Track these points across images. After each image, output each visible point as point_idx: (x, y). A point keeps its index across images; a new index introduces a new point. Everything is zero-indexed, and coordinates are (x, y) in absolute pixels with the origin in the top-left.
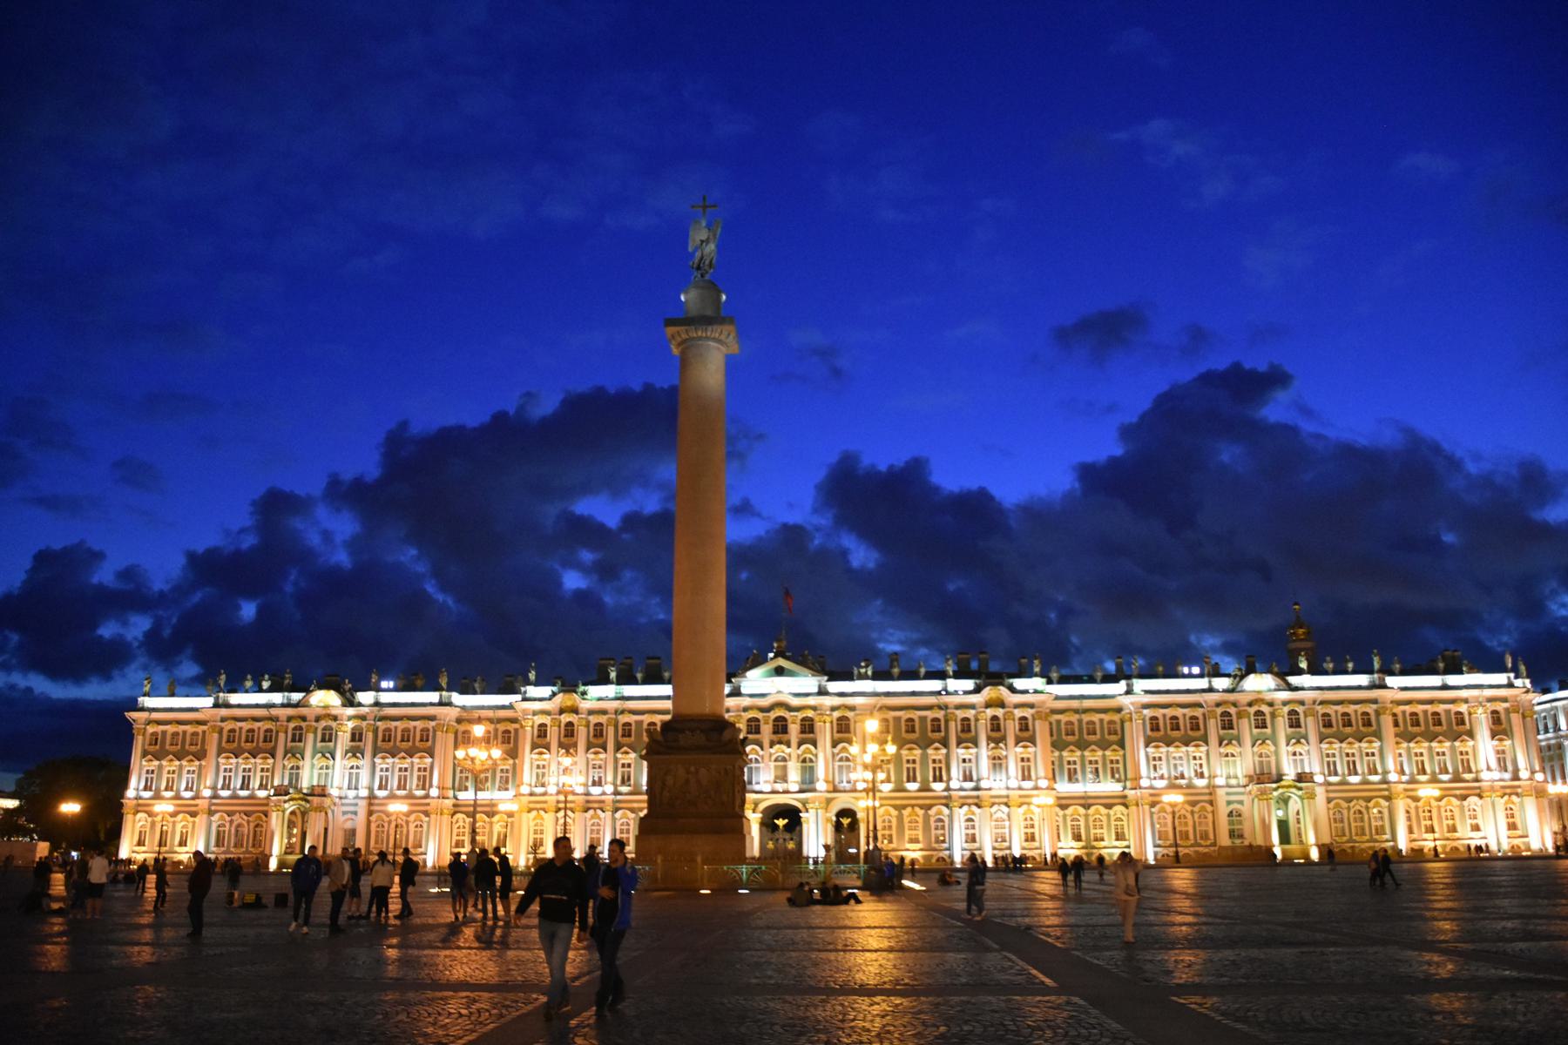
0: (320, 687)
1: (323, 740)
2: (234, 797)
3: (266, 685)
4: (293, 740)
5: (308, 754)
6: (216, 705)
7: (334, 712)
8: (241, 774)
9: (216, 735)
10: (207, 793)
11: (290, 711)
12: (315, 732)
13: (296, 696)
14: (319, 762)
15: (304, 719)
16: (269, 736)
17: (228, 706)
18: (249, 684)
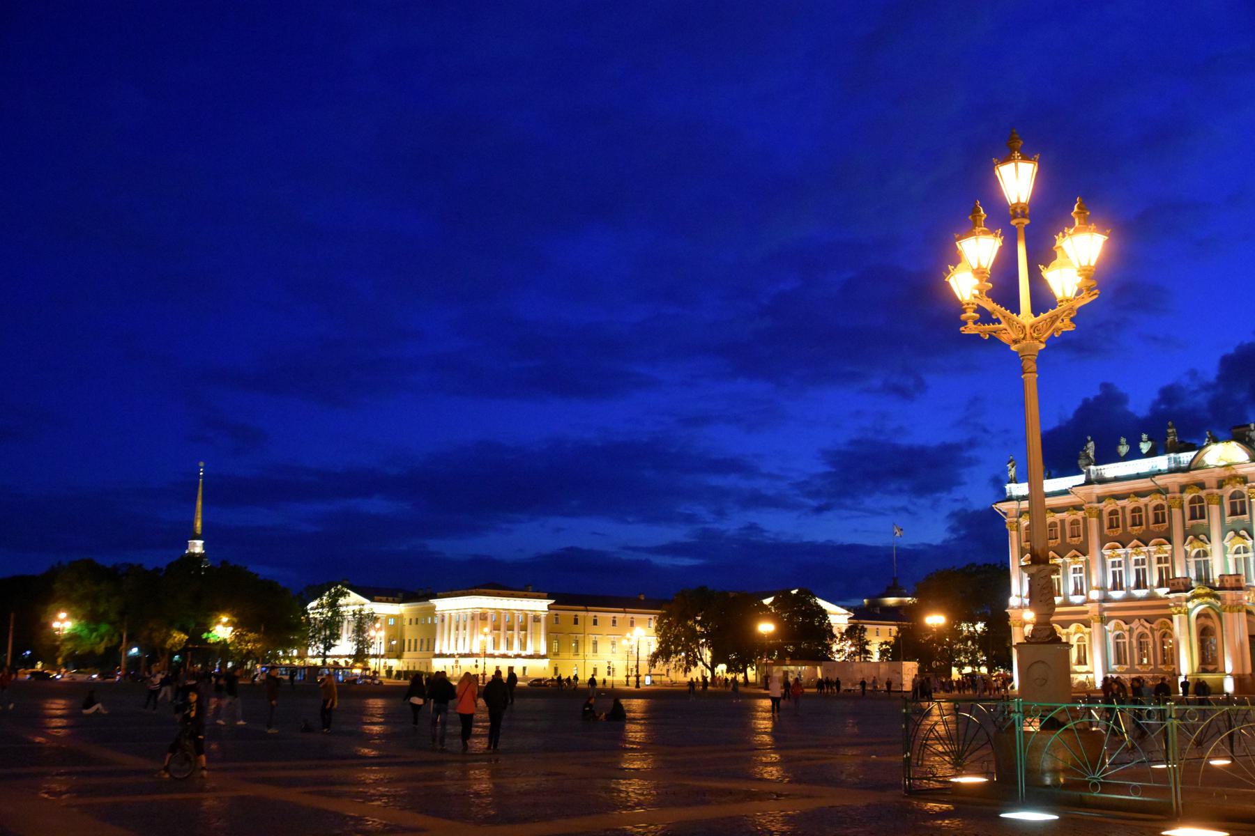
0: (1216, 441)
1: (1233, 513)
2: (1129, 598)
3: (1145, 447)
4: (1193, 517)
5: (1215, 533)
6: (1088, 482)
7: (1242, 471)
8: (1133, 569)
9: (1094, 522)
10: (1095, 595)
11: (1181, 478)
12: (1220, 503)
13: (1186, 457)
14: (1233, 543)
15: (1201, 485)
16: (1160, 515)
17: (1102, 481)
18: (1124, 449)
